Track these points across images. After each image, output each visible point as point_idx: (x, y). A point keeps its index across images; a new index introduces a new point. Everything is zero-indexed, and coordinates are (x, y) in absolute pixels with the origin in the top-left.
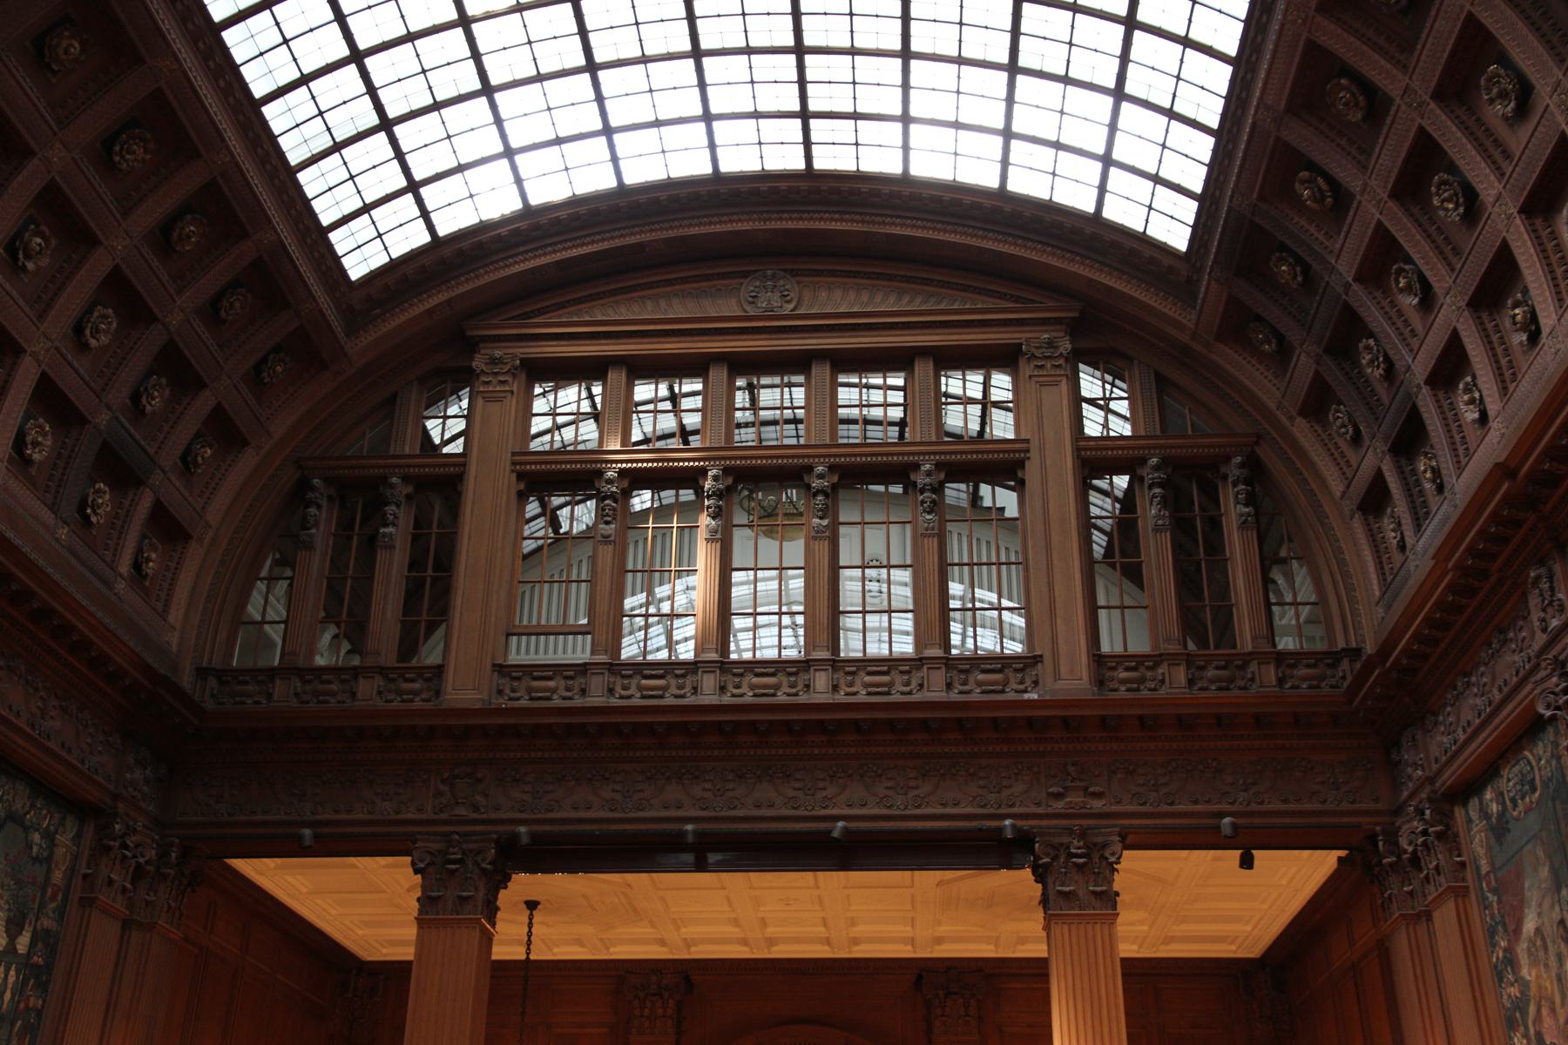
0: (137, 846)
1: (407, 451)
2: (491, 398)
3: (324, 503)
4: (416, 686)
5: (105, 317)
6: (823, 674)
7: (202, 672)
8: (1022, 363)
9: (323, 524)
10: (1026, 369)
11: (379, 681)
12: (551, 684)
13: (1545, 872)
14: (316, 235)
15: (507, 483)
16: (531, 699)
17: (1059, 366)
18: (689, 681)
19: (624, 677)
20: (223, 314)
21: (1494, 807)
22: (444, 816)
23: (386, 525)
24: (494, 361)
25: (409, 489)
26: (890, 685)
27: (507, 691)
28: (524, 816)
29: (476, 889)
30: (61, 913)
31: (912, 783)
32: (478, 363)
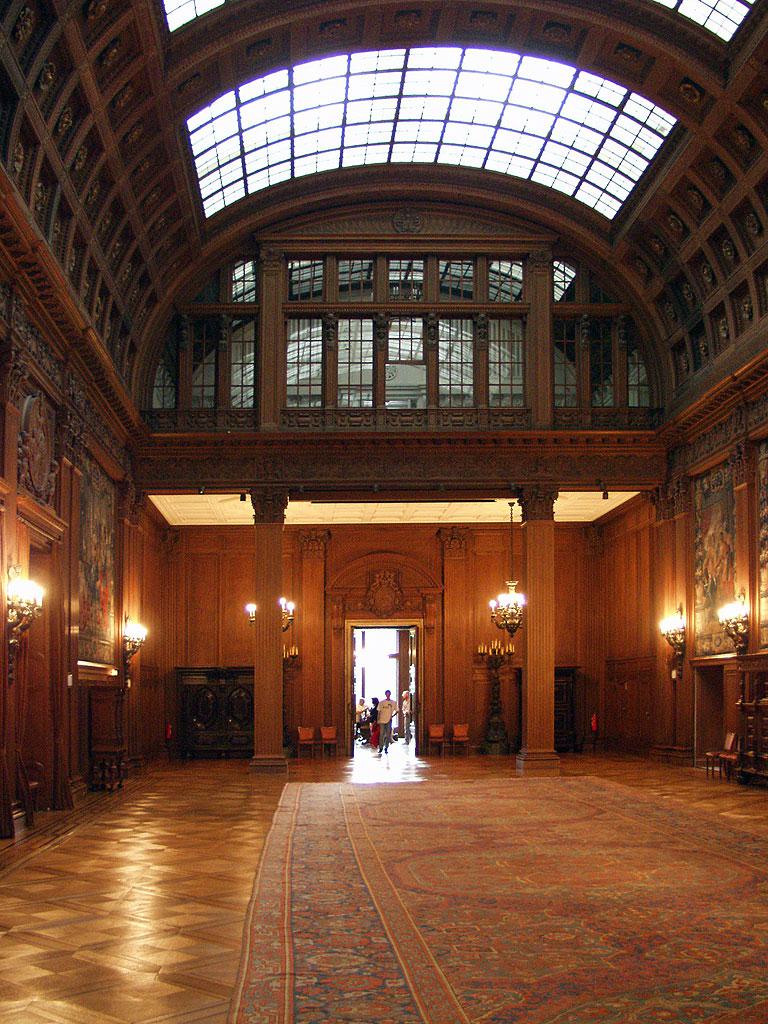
11: (227, 417)
13: (720, 515)
15: (281, 317)
21: (706, 486)
22: (262, 480)
23: (222, 339)
24: (270, 253)
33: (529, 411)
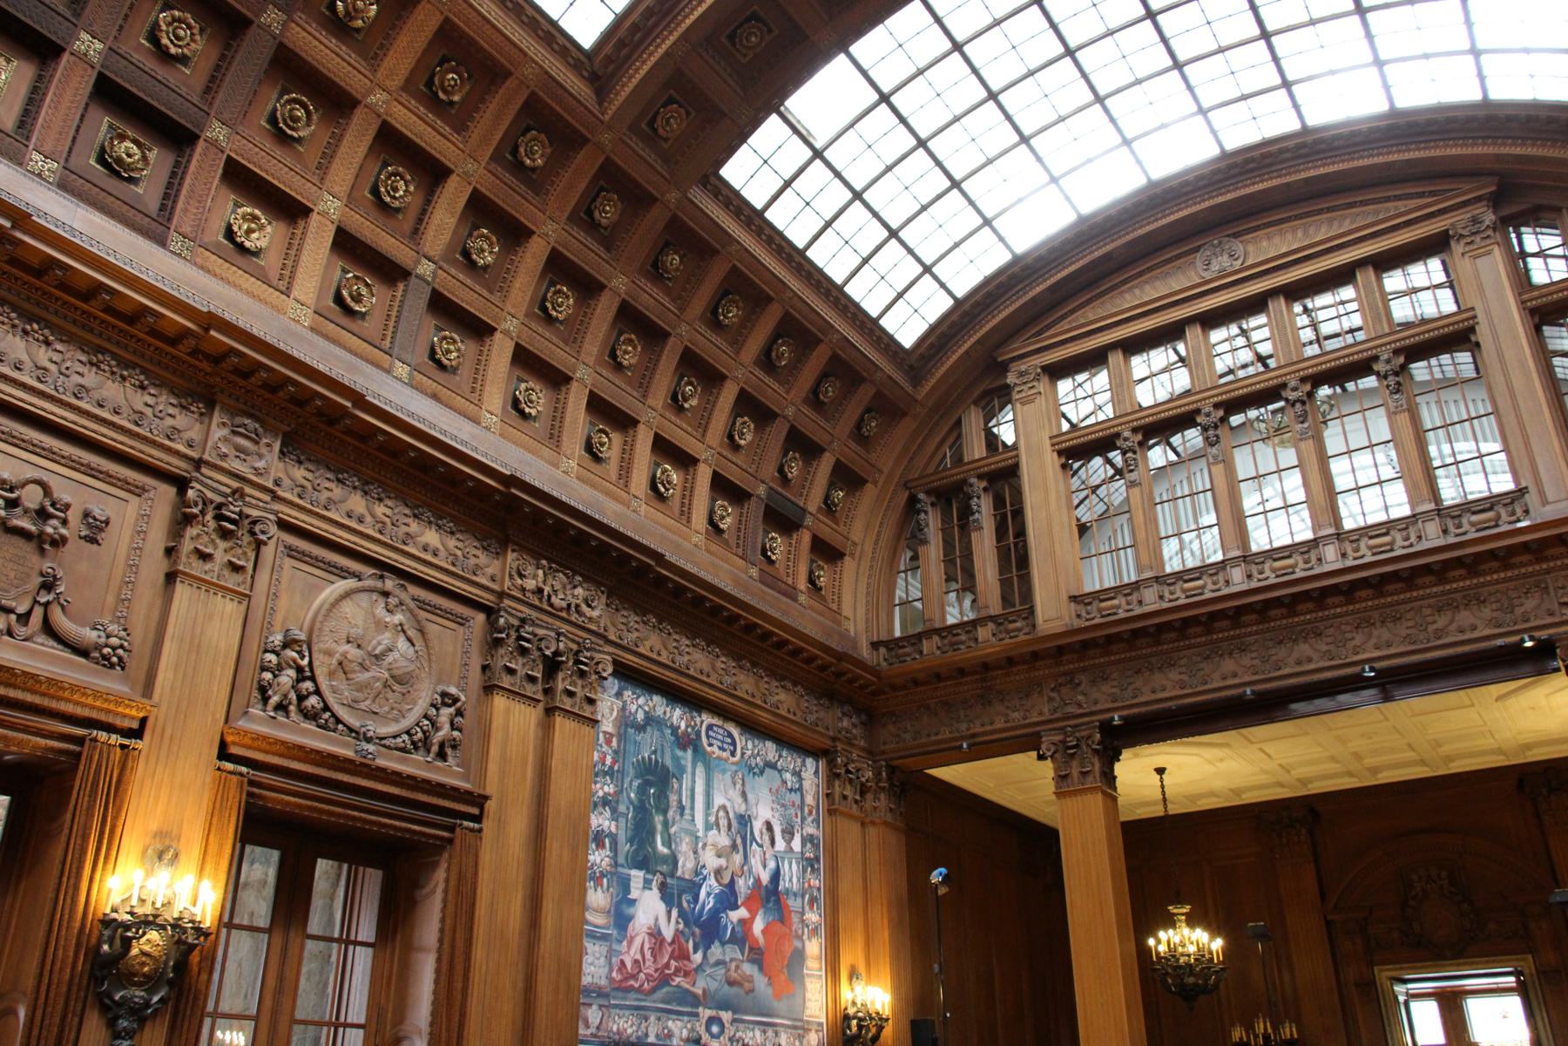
0: (858, 771)
1: (977, 457)
2: (1026, 401)
3: (929, 509)
4: (1018, 624)
5: (745, 423)
6: (1331, 547)
7: (875, 645)
8: (1453, 243)
9: (932, 521)
10: (1457, 248)
12: (1115, 602)
14: (869, 326)
15: (1052, 461)
16: (1103, 616)
17: (1488, 237)
18: (1221, 577)
19: (1169, 585)
20: (821, 397)
24: (1021, 374)
25: (984, 484)
26: (1392, 543)
27: (1084, 614)
28: (1116, 705)
29: (1093, 764)
30: (817, 820)
31: (1430, 619)
32: (1011, 379)
33: (1520, 492)
